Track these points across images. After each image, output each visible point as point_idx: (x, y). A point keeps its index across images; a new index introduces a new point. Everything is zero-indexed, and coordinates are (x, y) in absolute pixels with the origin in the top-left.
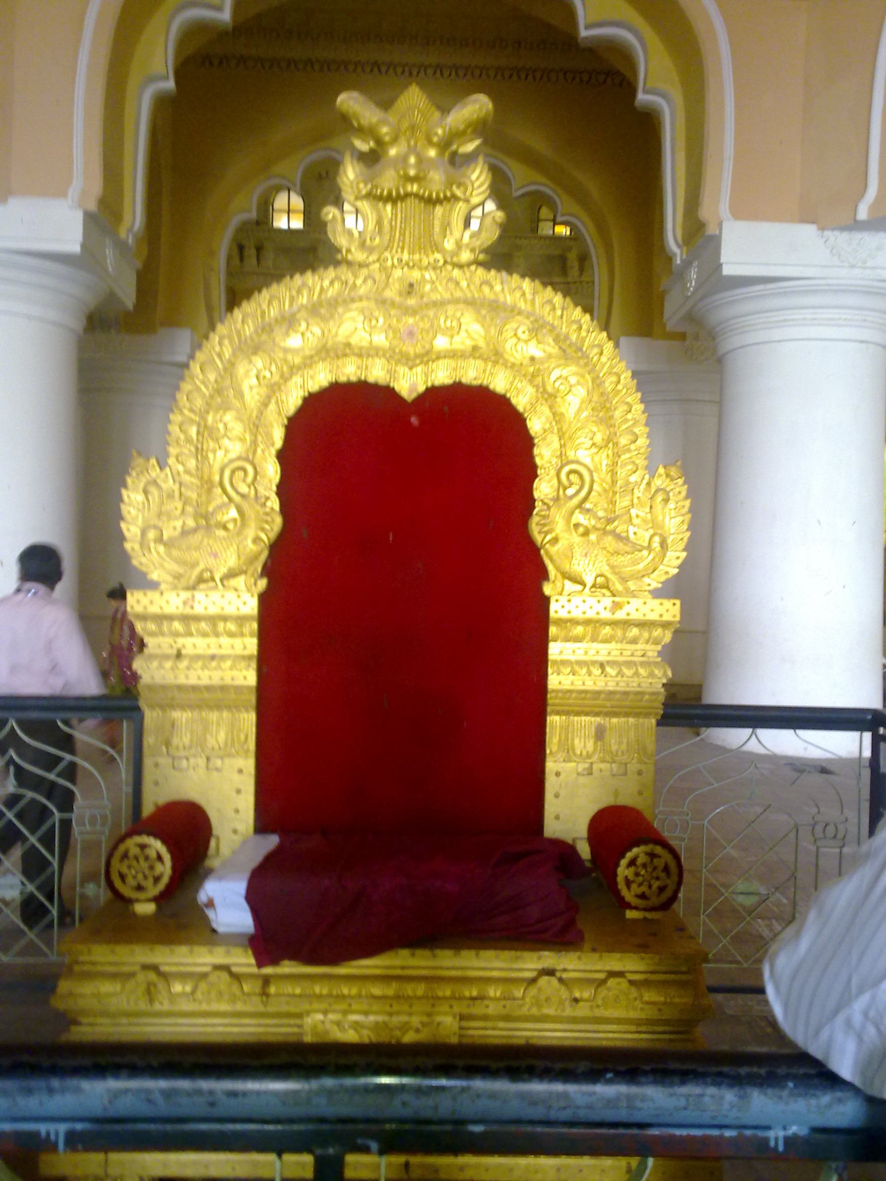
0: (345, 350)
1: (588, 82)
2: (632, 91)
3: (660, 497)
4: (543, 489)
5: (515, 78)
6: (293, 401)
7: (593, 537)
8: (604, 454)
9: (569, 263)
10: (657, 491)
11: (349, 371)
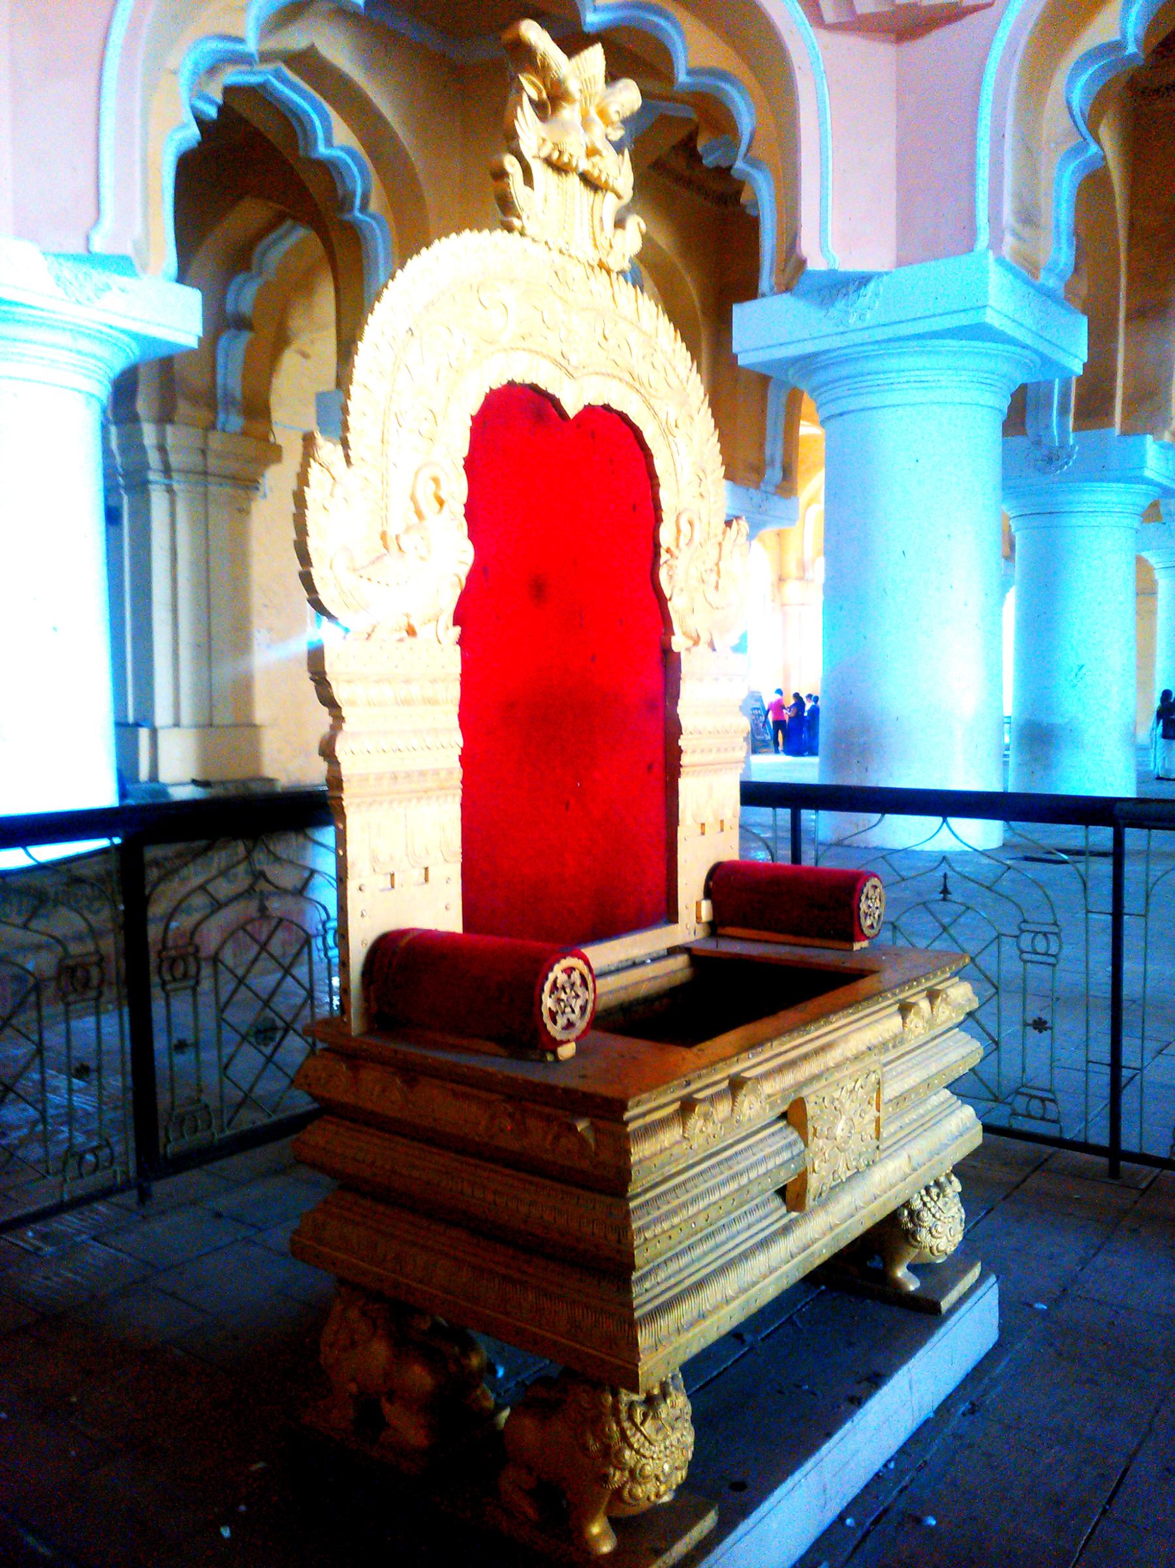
4: (666, 534)
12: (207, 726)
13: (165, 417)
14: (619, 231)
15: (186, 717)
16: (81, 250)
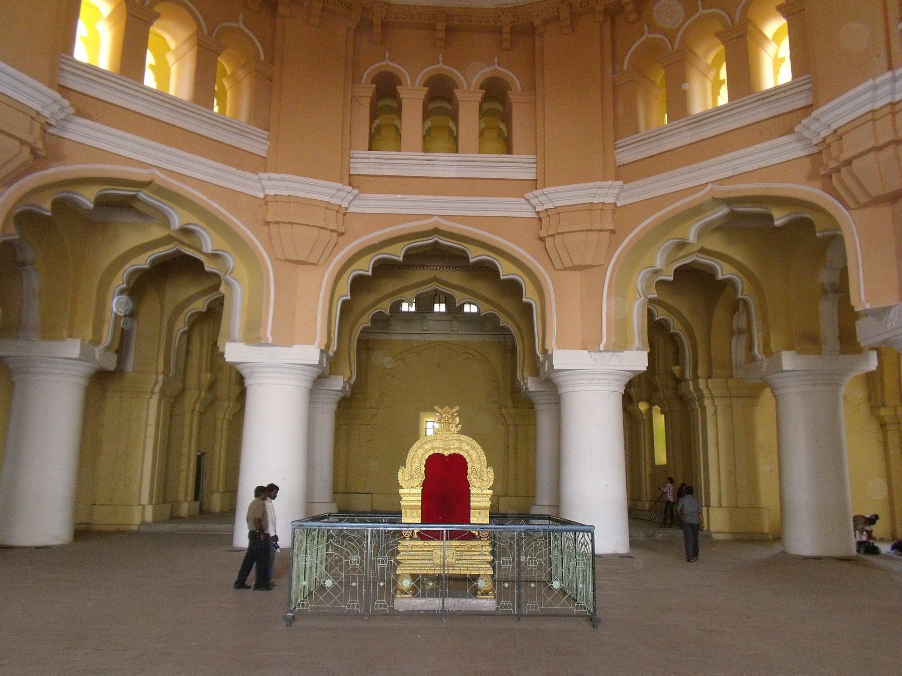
0: (436, 448)
4: (469, 471)
6: (427, 457)
11: (436, 451)
12: (734, 508)
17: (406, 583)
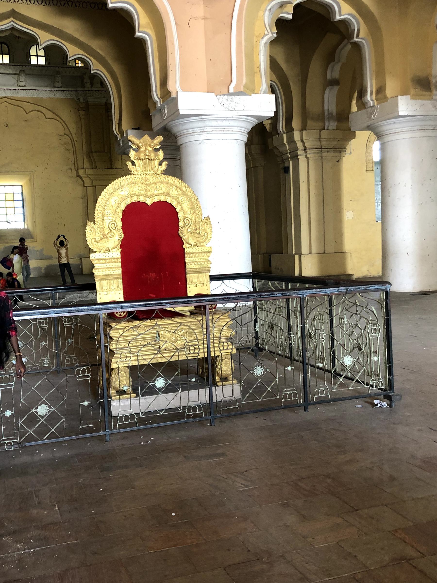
1: (102, 8)
2: (134, 33)
3: (206, 224)
4: (181, 224)
5: (66, 5)
6: (123, 207)
7: (192, 234)
8: (193, 215)
9: (85, 81)
10: (205, 222)
12: (323, 254)
13: (304, 128)
14: (160, 166)
15: (314, 251)
16: (227, 93)
17: (121, 380)
